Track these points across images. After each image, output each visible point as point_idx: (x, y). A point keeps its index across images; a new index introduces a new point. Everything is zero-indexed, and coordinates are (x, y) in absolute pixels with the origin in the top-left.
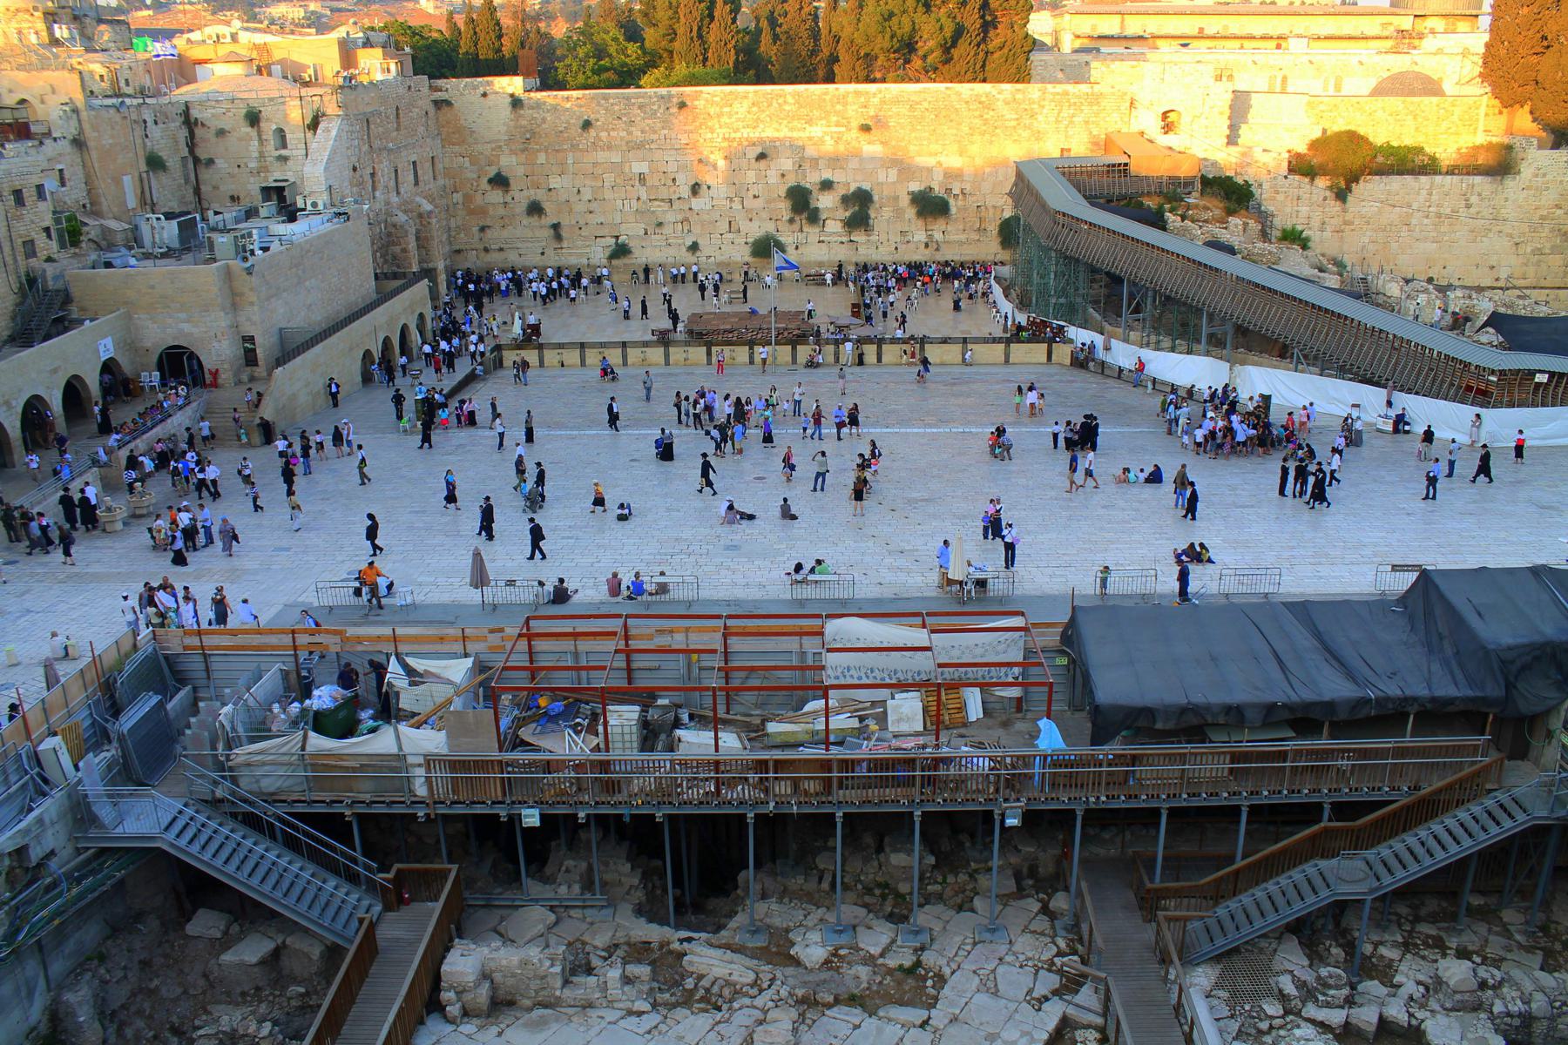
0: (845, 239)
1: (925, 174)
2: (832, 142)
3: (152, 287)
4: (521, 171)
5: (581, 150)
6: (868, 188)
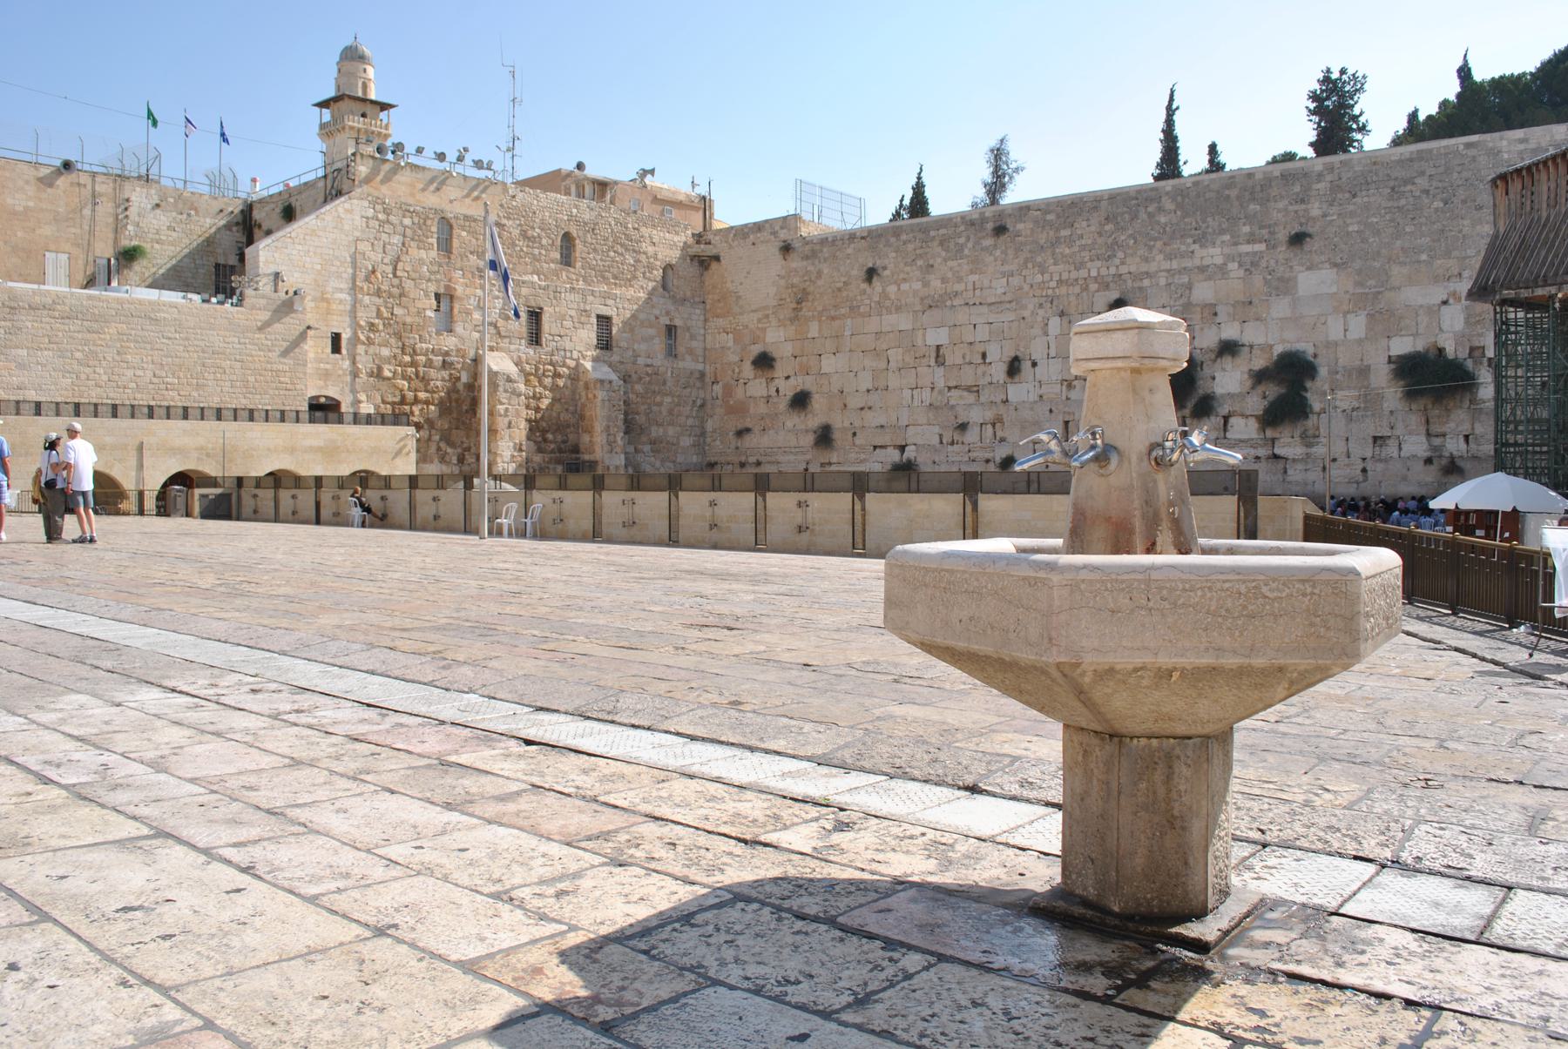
0: (1262, 452)
1: (1423, 319)
2: (1241, 273)
5: (863, 315)
6: (1310, 350)
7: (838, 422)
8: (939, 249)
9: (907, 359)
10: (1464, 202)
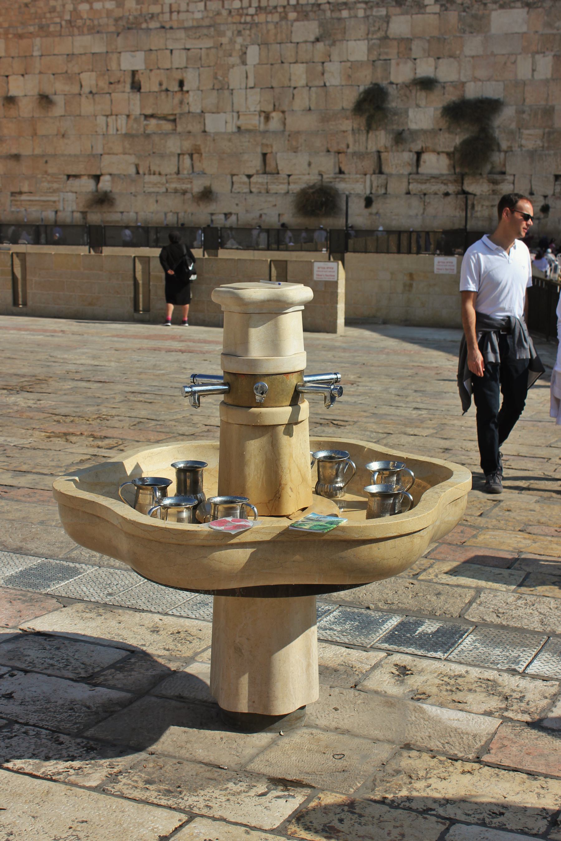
2: (437, 8)
9: (101, 84)
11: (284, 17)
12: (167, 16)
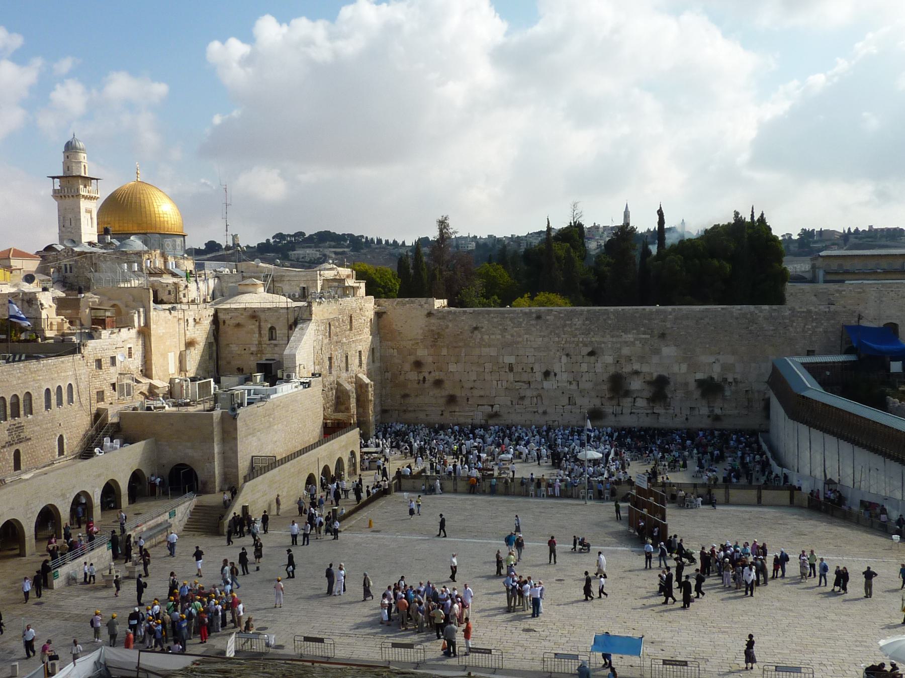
0: (649, 411)
2: (640, 345)
3: (172, 424)
4: (430, 359)
7: (458, 393)
8: (510, 322)
9: (494, 368)
10: (721, 328)
11: (578, 345)
12: (525, 343)
